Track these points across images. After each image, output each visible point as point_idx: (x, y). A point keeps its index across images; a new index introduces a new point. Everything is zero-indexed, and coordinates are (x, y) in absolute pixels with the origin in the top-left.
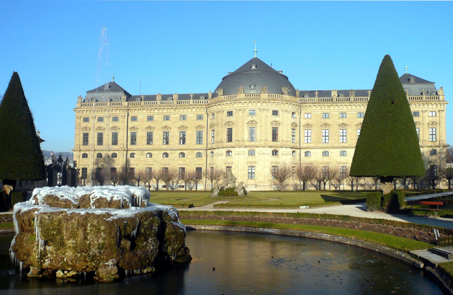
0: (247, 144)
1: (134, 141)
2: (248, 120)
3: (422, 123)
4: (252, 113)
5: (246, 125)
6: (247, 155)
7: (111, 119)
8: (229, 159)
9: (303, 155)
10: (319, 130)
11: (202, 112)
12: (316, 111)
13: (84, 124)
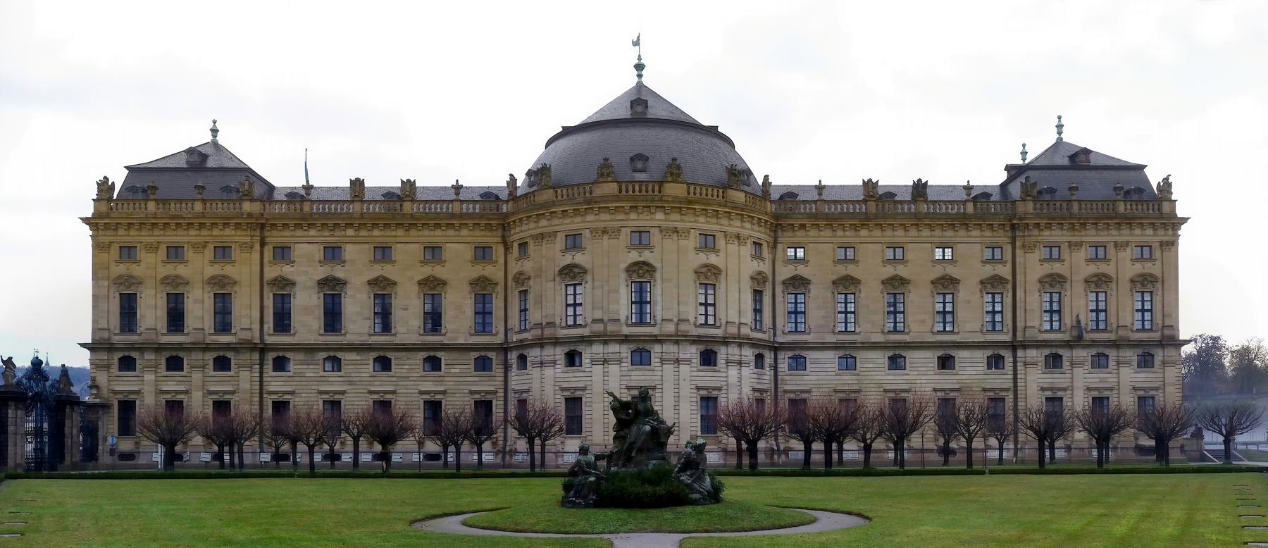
0: (626, 330)
1: (283, 321)
2: (629, 261)
3: (1114, 276)
4: (641, 239)
5: (623, 275)
6: (626, 364)
7: (209, 253)
8: (574, 378)
9: (784, 366)
10: (829, 295)
11: (492, 239)
12: (821, 240)
13: (121, 269)
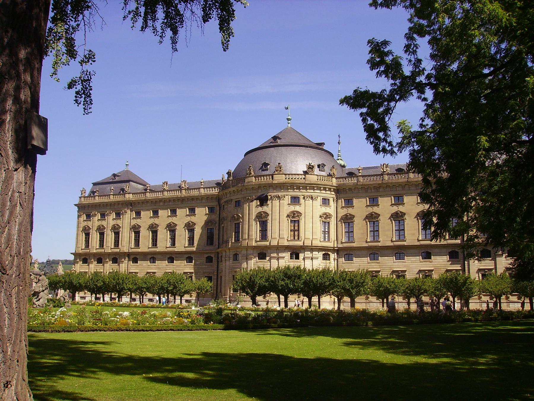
11: (214, 204)
